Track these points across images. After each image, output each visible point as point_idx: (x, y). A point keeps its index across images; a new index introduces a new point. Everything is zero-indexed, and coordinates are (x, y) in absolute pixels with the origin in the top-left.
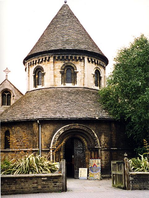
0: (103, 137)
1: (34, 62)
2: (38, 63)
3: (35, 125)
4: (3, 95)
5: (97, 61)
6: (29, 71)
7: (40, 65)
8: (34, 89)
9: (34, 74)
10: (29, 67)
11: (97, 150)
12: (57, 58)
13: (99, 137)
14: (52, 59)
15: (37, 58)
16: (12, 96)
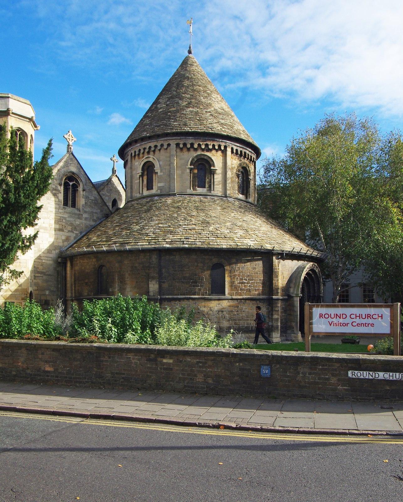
4: (66, 185)
7: (208, 154)
9: (192, 167)
10: (176, 151)
15: (202, 141)
16: (80, 189)
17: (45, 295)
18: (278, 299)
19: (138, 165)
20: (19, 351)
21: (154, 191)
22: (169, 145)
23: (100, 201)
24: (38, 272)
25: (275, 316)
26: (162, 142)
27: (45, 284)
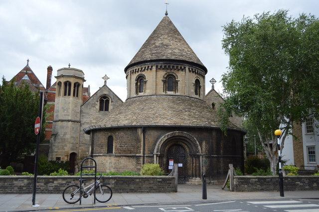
0: (204, 144)
1: (137, 70)
2: (141, 71)
4: (101, 102)
5: (198, 71)
6: (131, 78)
7: (143, 73)
8: (135, 96)
11: (198, 157)
12: (159, 67)
13: (201, 145)
14: (154, 68)
16: (110, 102)
18: (140, 156)
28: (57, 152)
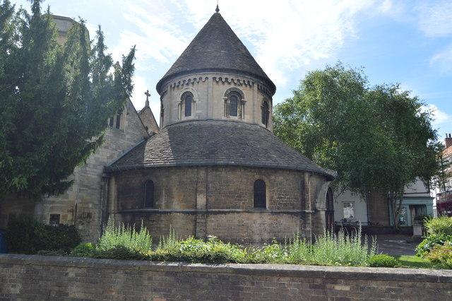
3: (307, 175)
7: (239, 88)
8: (224, 118)
14: (256, 85)
16: (125, 112)
17: (88, 208)
19: (177, 95)
20: (114, 275)
21: (191, 117)
22: (207, 78)
23: (140, 124)
24: (84, 186)
25: (308, 229)
26: (200, 76)
27: (89, 197)
28: (53, 202)
